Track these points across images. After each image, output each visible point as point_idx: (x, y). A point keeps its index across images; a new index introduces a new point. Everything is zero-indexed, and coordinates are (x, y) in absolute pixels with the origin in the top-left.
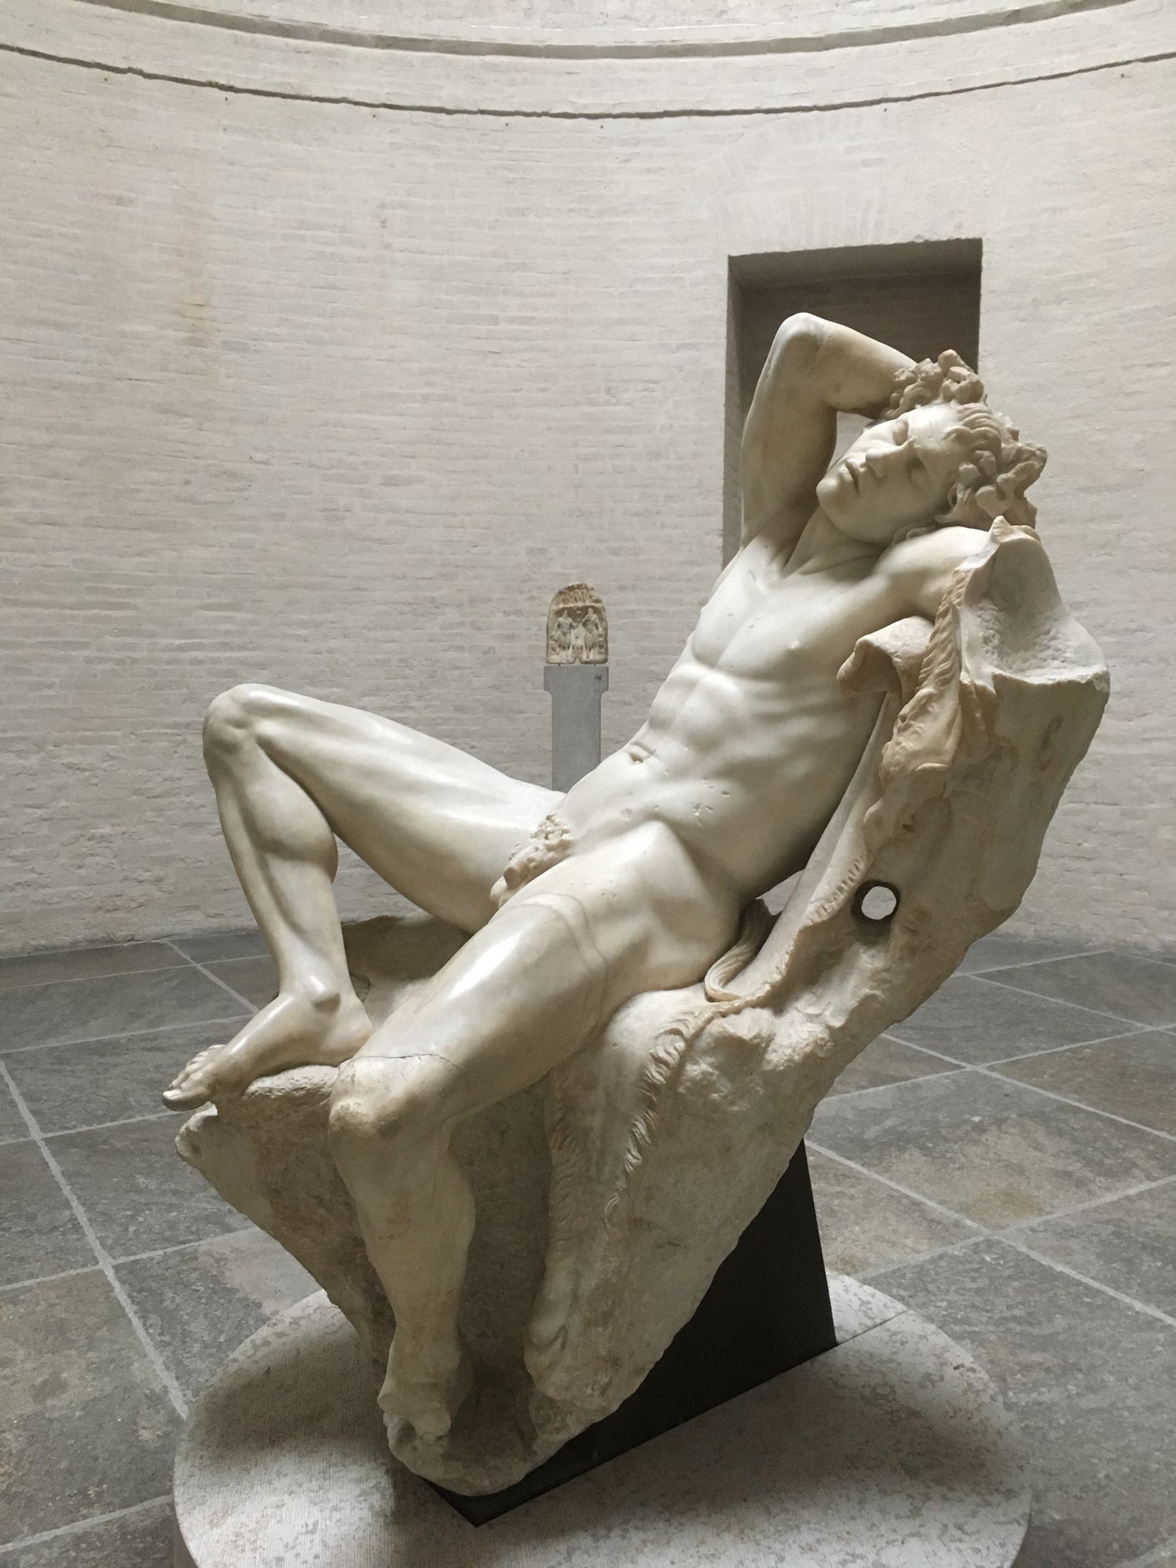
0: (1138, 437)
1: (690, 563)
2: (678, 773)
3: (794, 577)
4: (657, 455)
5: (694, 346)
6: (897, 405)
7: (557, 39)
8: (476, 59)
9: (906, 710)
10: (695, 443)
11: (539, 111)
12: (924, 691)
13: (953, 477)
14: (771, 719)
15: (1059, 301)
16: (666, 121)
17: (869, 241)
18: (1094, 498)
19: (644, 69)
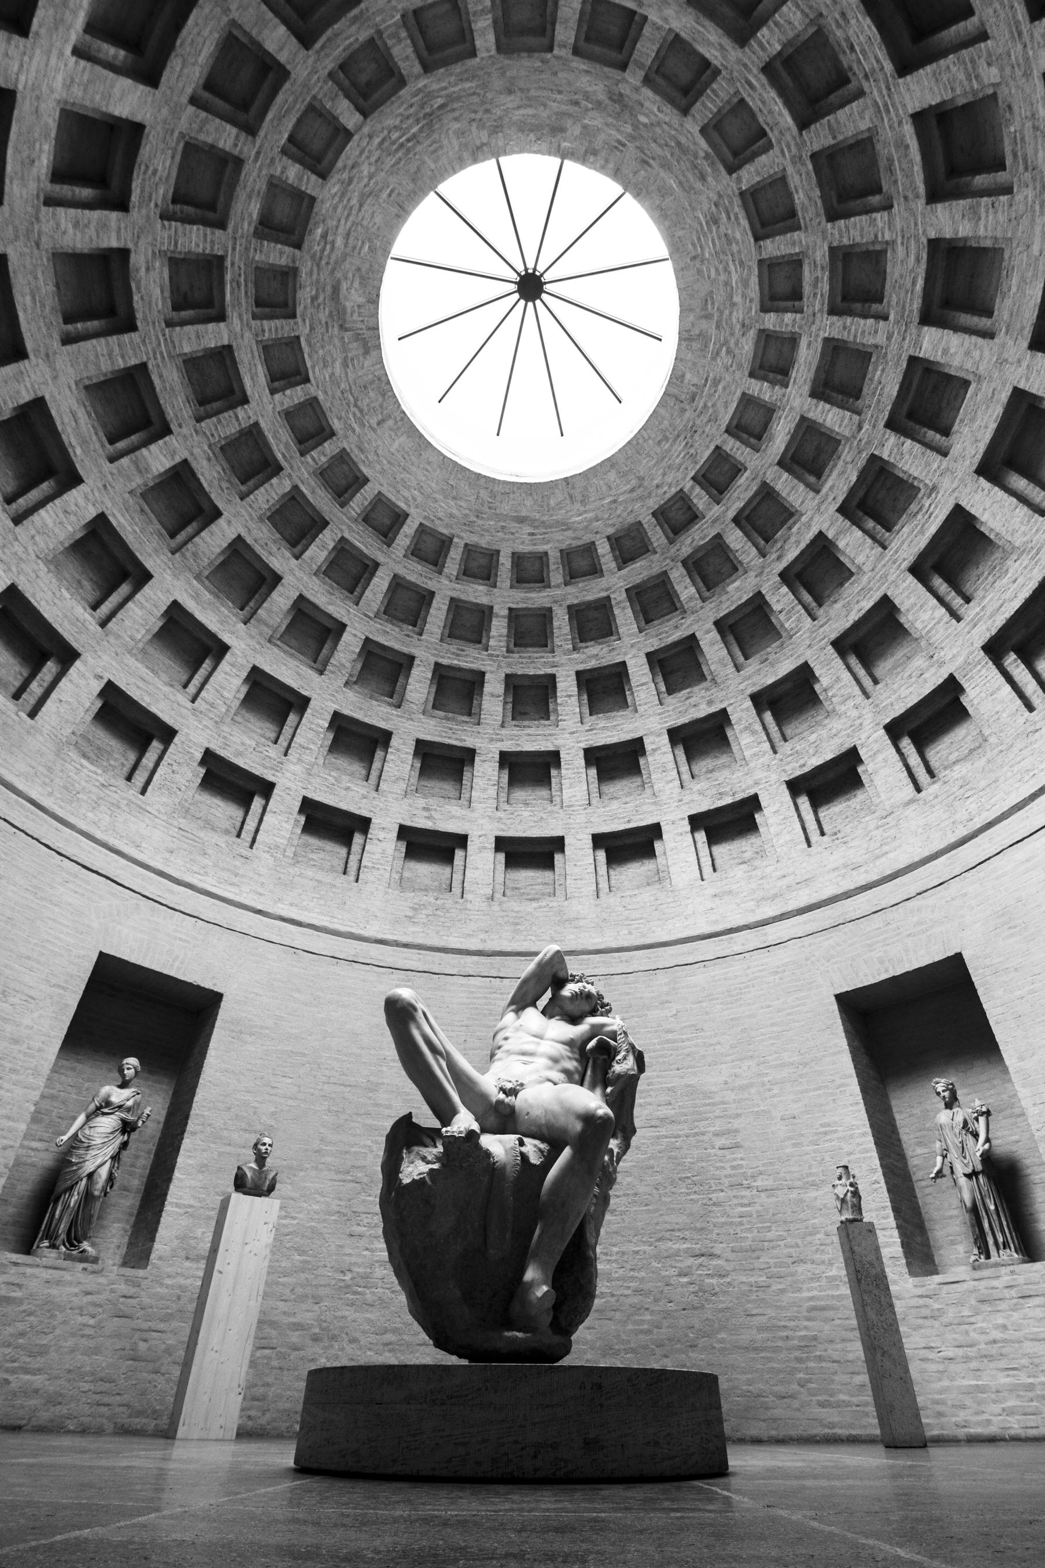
0: (273, 1109)
1: (9, 1118)
2: (550, 1068)
3: (553, 1020)
4: (16, 1042)
5: (64, 988)
6: (572, 981)
7: (60, 813)
8: (14, 796)
9: (618, 1058)
10: (43, 1043)
11: (35, 836)
12: (623, 1053)
13: (597, 1004)
14: (570, 1058)
15: (251, 1034)
16: (95, 875)
17: (172, 974)
18: (247, 1136)
19: (94, 849)
